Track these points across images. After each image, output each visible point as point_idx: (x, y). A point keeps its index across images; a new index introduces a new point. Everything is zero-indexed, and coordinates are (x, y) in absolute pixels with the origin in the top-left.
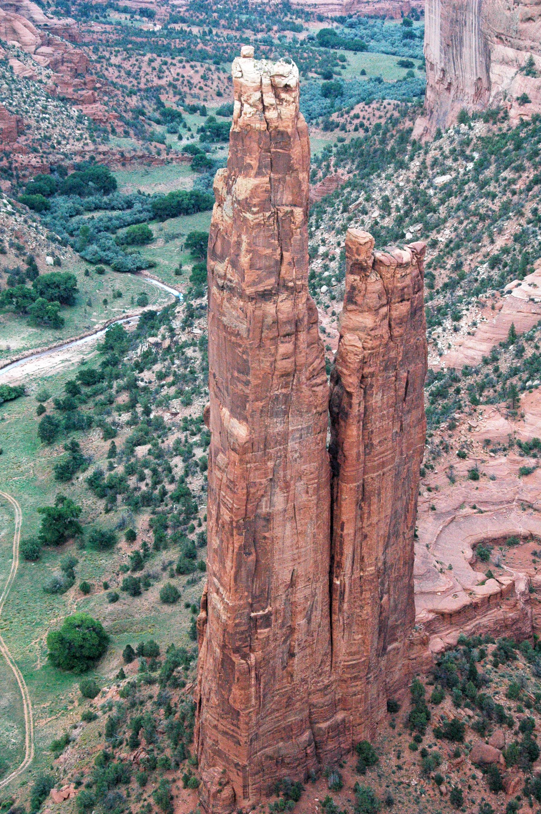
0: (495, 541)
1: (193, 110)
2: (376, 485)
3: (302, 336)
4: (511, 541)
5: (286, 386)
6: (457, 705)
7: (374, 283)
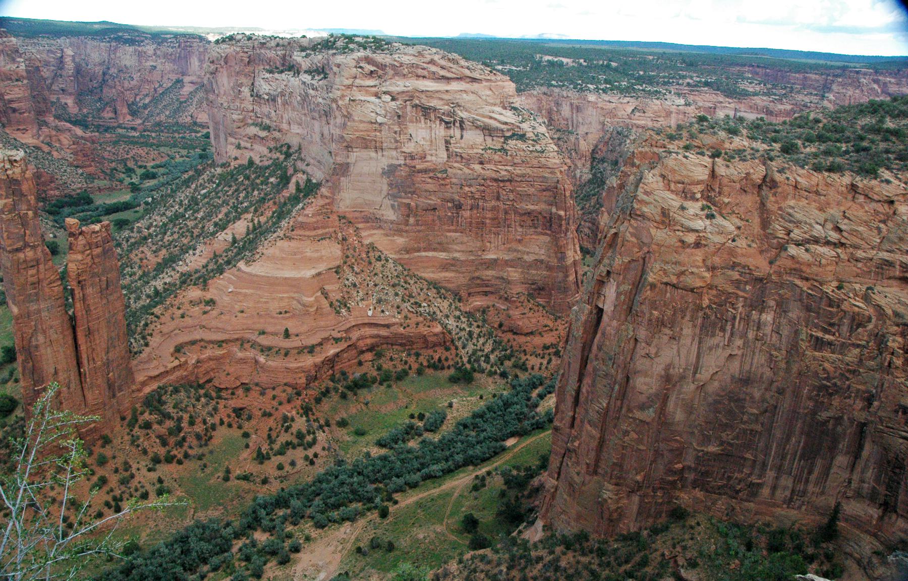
0: (186, 343)
1: (140, 167)
2: (96, 326)
3: (41, 266)
4: (193, 343)
5: (35, 288)
6: (151, 414)
7: (81, 241)
